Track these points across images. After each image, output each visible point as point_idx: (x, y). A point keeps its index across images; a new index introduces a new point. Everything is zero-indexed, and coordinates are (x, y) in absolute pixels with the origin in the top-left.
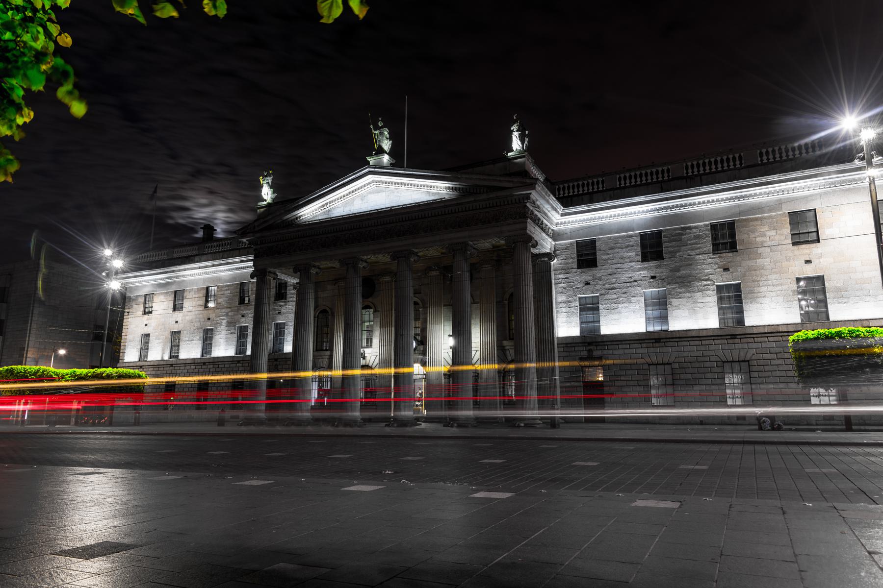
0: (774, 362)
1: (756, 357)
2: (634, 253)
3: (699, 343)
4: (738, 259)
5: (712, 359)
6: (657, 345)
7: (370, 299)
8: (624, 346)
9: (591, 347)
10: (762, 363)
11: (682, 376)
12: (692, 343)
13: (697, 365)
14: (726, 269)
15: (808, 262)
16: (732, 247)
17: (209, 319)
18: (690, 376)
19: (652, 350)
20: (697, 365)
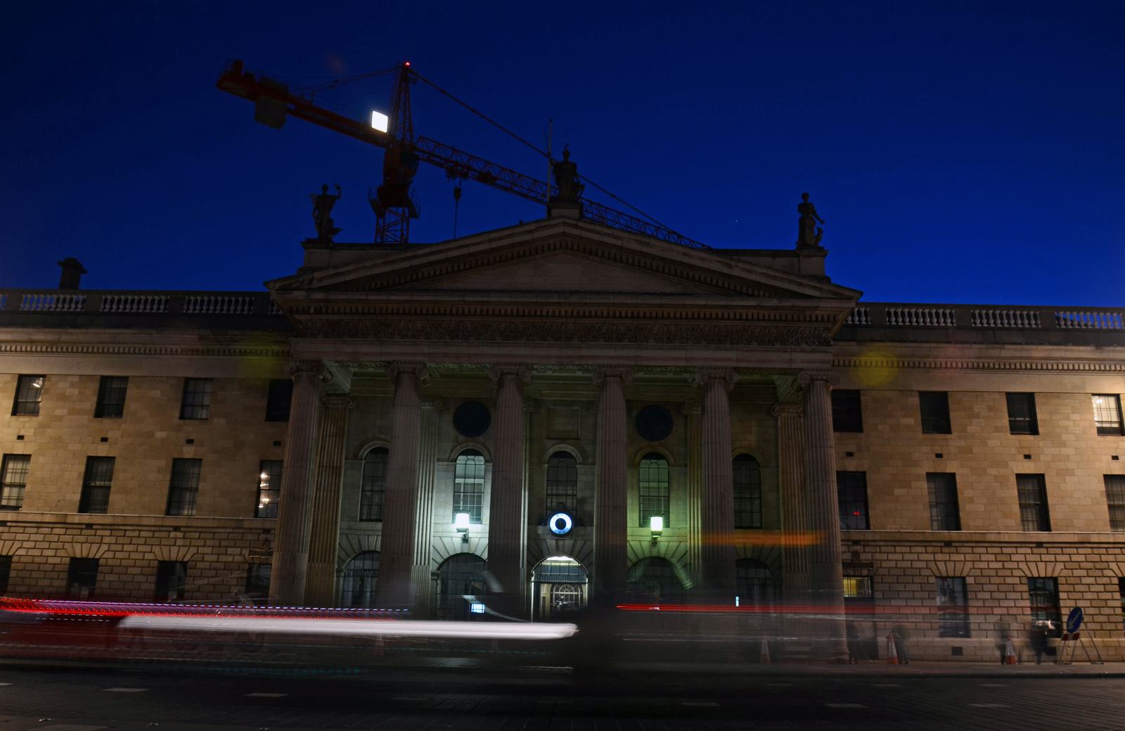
0: (1085, 581)
1: (1065, 573)
2: (913, 421)
3: (997, 550)
4: (1041, 444)
5: (1016, 573)
6: (946, 550)
7: (481, 438)
8: (903, 549)
9: (857, 548)
10: (1072, 580)
11: (980, 595)
12: (990, 550)
13: (997, 580)
14: (1028, 457)
15: (1115, 458)
16: (1034, 430)
17: (104, 440)
18: (987, 596)
19: (939, 557)
20: (997, 580)
